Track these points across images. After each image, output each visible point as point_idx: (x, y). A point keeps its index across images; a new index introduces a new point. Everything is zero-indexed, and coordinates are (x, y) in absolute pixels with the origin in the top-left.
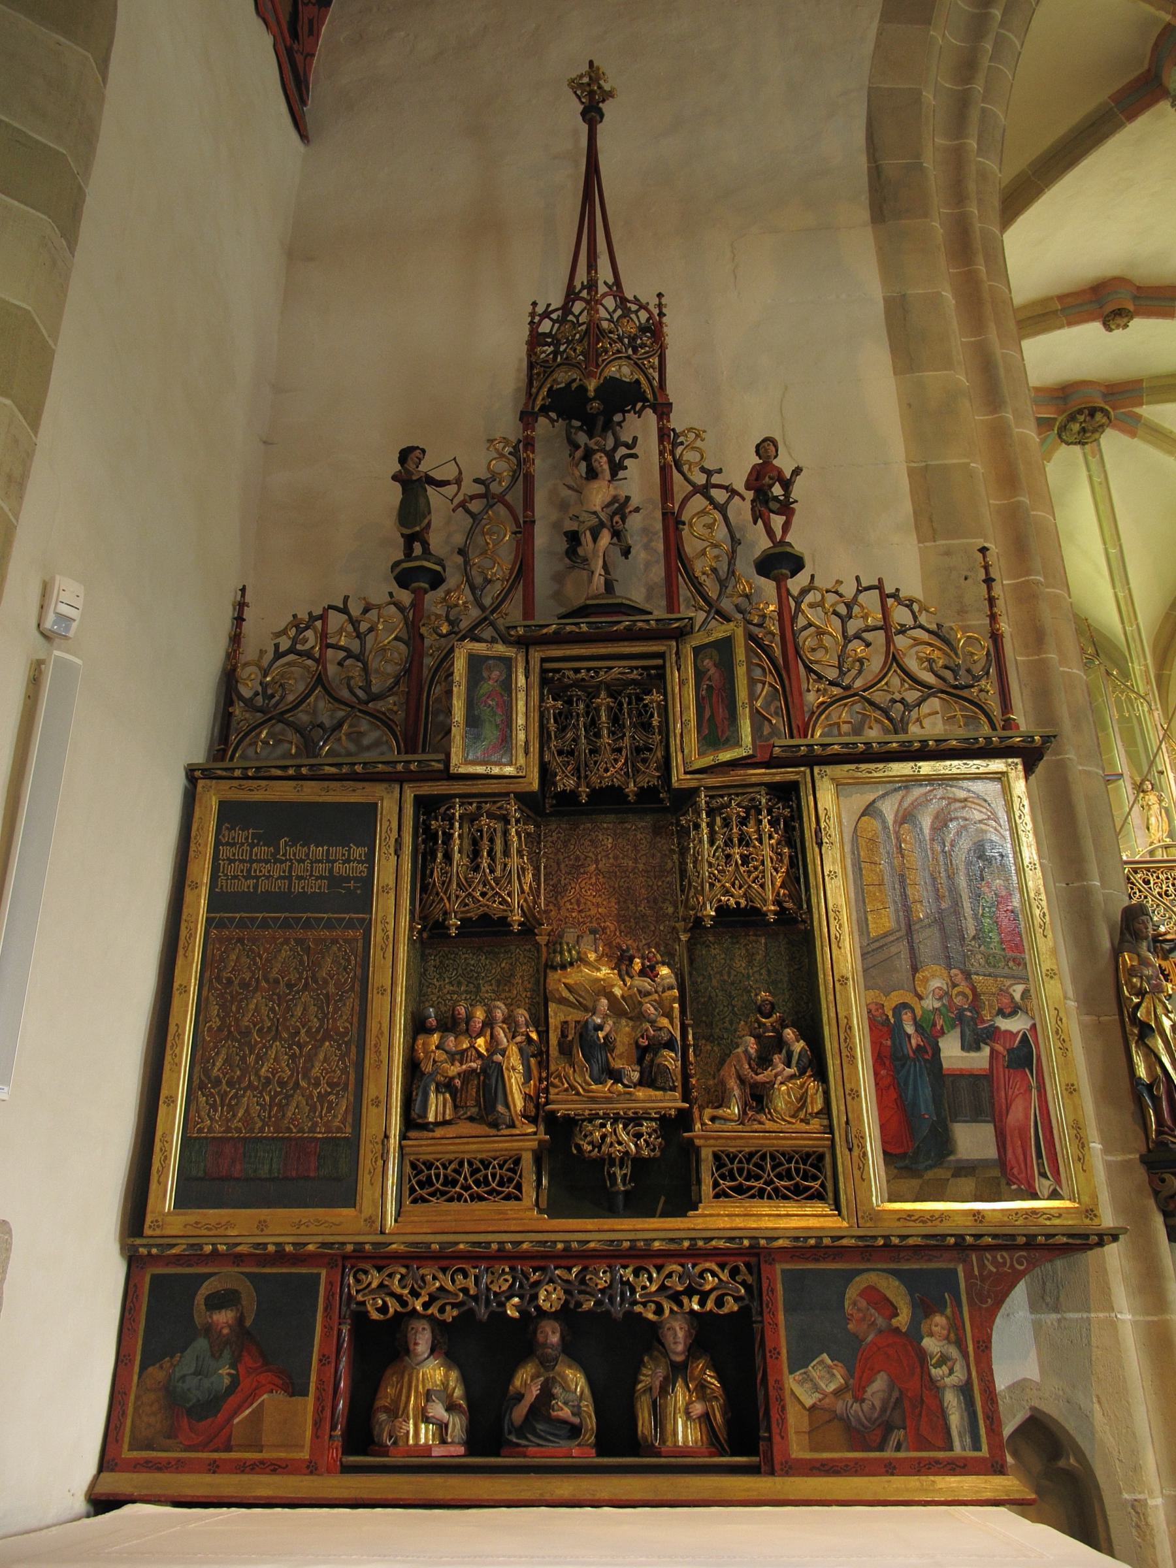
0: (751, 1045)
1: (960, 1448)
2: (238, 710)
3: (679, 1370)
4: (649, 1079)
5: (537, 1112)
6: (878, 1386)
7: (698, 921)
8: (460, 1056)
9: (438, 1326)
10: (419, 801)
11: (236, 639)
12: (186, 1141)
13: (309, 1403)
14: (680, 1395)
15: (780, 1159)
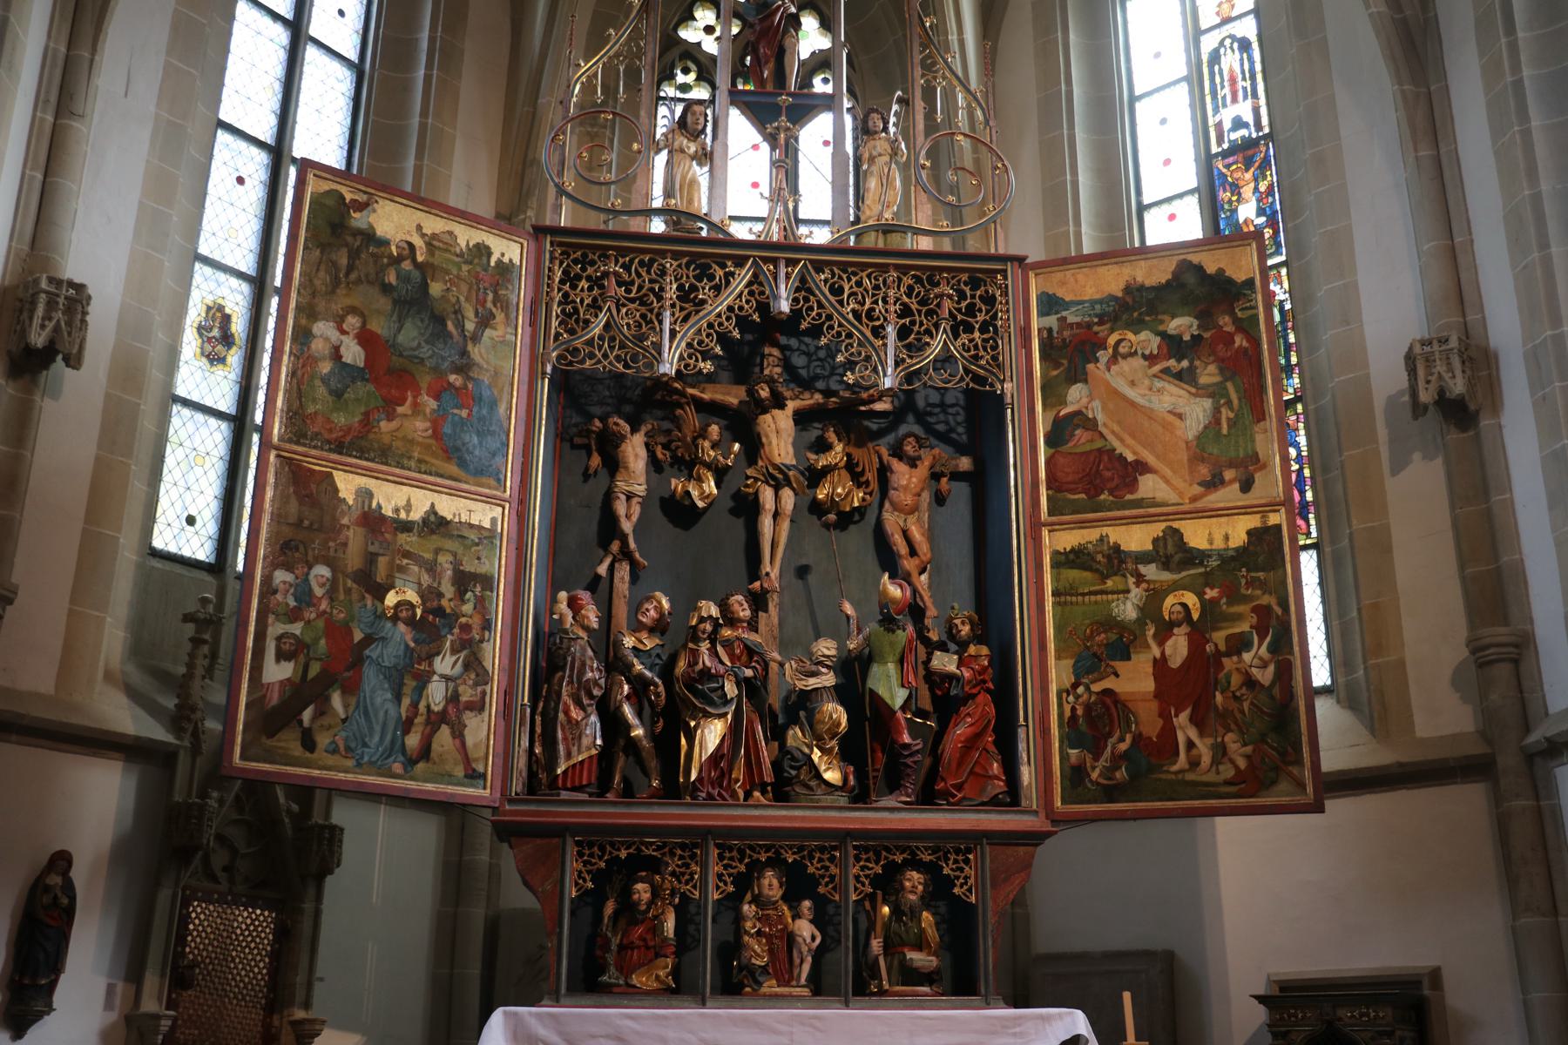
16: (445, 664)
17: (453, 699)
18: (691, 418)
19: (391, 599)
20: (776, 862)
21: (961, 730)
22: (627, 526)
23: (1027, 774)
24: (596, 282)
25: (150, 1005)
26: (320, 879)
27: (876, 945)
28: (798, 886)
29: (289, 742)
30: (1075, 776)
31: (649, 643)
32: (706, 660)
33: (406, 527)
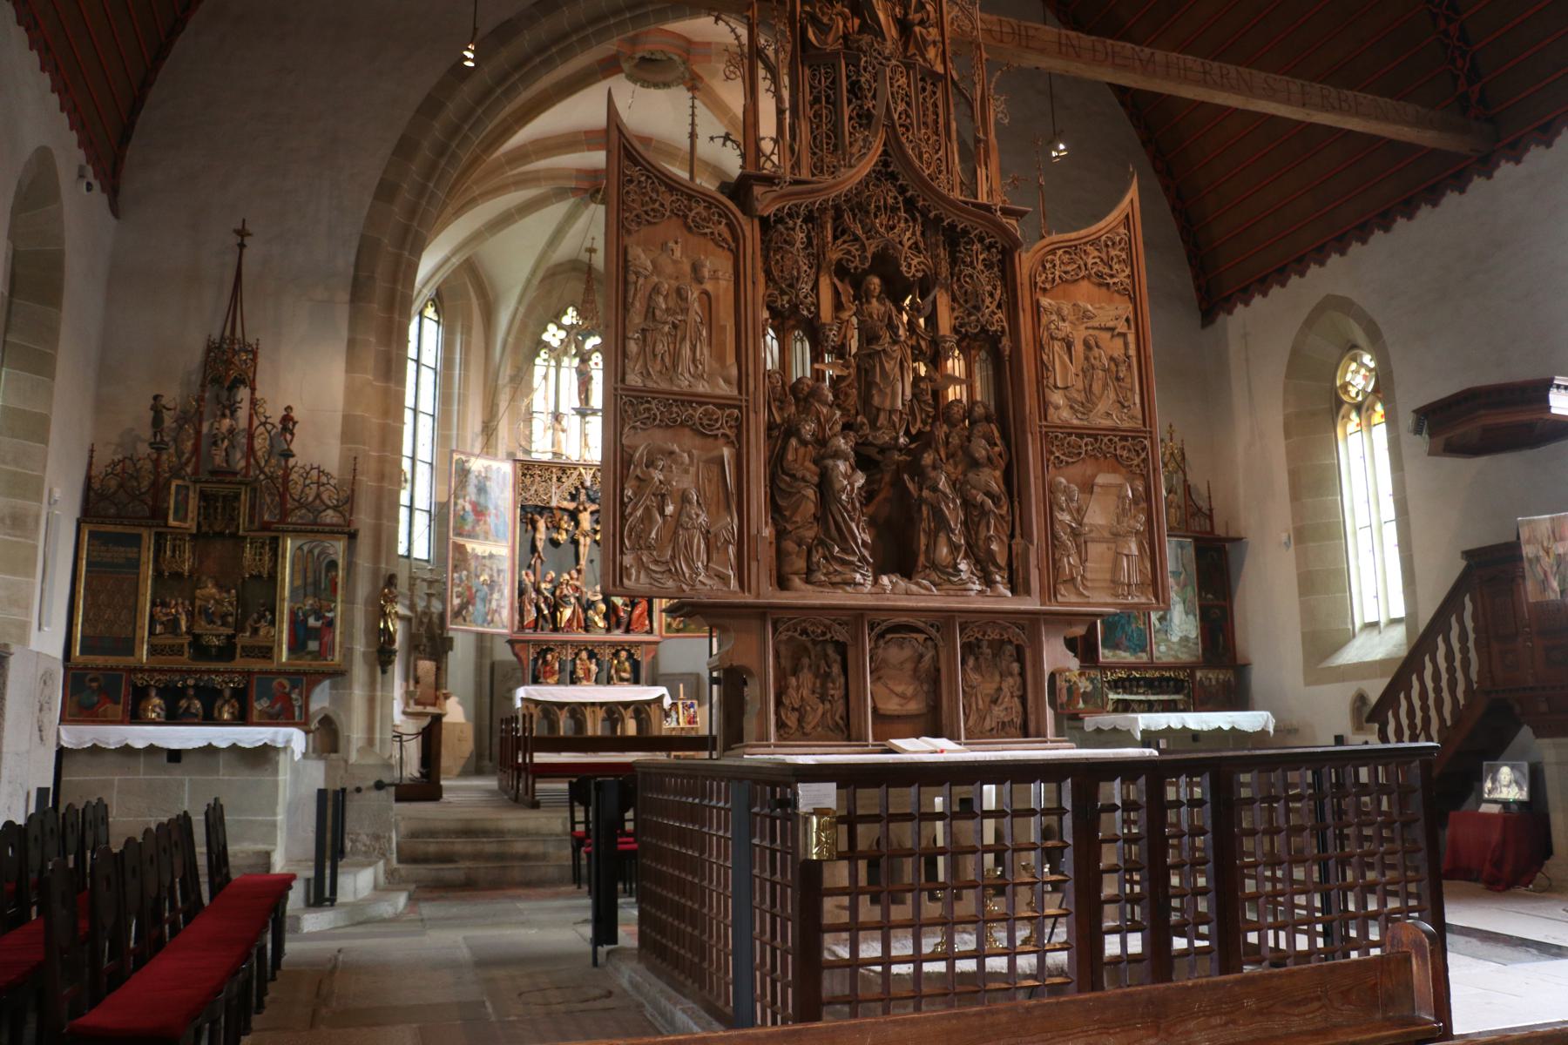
0: (255, 616)
1: (297, 720)
2: (92, 494)
3: (227, 702)
4: (224, 624)
5: (189, 631)
6: (278, 706)
7: (243, 578)
8: (167, 614)
9: (158, 689)
10: (156, 533)
11: (90, 465)
12: (82, 636)
13: (121, 707)
14: (226, 708)
15: (260, 648)
16: (496, 596)
17: (498, 606)
18: (558, 514)
19: (482, 579)
20: (586, 649)
21: (637, 612)
22: (540, 549)
23: (655, 625)
24: (532, 476)
25: (412, 688)
26: (446, 653)
27: (613, 671)
28: (591, 655)
29: (460, 619)
30: (669, 626)
31: (549, 586)
32: (565, 592)
33: (484, 557)
